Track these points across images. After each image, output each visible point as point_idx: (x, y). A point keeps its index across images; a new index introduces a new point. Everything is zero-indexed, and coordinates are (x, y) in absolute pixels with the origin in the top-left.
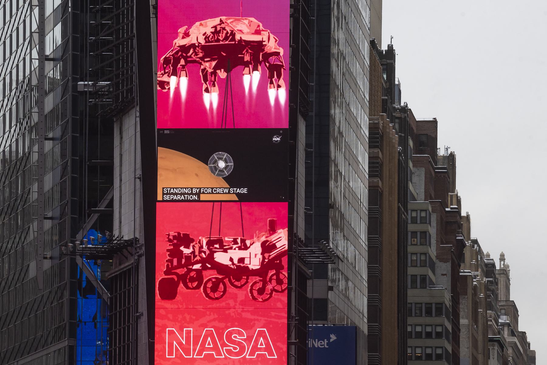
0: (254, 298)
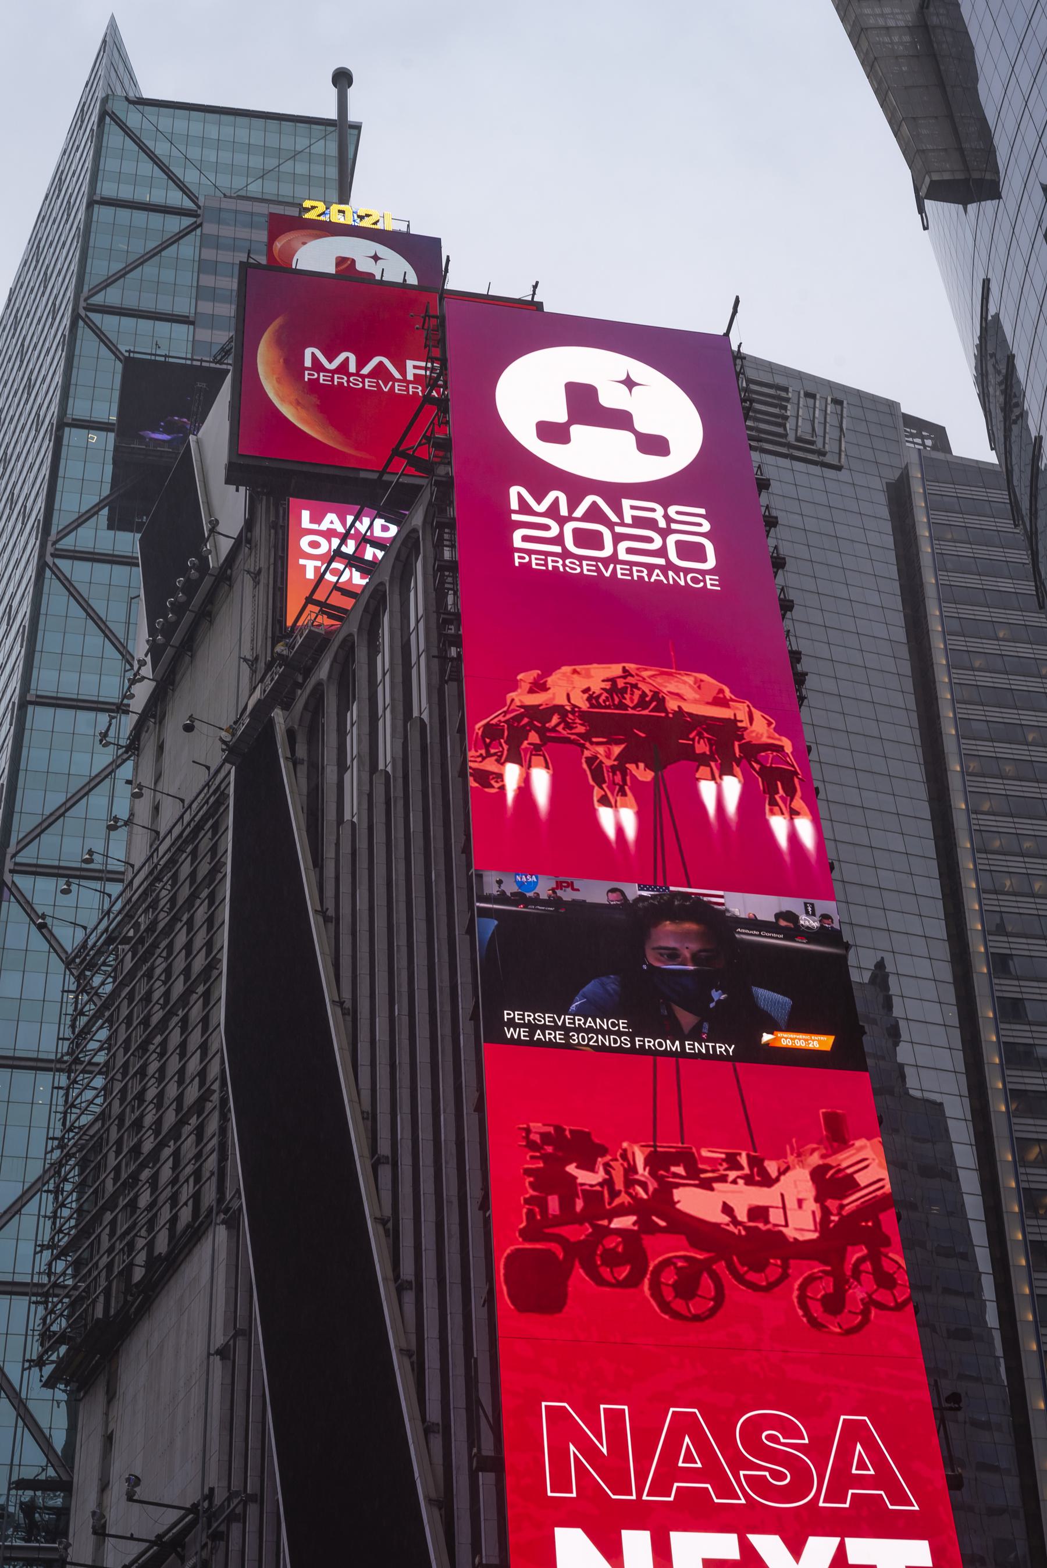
0: (813, 1322)
